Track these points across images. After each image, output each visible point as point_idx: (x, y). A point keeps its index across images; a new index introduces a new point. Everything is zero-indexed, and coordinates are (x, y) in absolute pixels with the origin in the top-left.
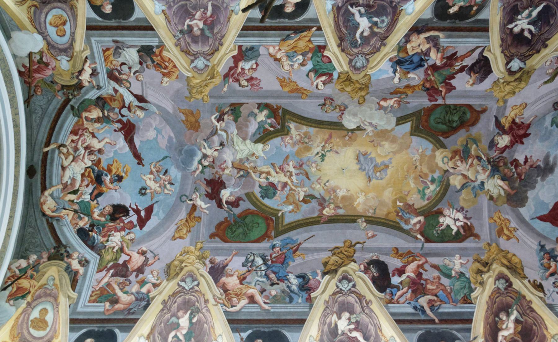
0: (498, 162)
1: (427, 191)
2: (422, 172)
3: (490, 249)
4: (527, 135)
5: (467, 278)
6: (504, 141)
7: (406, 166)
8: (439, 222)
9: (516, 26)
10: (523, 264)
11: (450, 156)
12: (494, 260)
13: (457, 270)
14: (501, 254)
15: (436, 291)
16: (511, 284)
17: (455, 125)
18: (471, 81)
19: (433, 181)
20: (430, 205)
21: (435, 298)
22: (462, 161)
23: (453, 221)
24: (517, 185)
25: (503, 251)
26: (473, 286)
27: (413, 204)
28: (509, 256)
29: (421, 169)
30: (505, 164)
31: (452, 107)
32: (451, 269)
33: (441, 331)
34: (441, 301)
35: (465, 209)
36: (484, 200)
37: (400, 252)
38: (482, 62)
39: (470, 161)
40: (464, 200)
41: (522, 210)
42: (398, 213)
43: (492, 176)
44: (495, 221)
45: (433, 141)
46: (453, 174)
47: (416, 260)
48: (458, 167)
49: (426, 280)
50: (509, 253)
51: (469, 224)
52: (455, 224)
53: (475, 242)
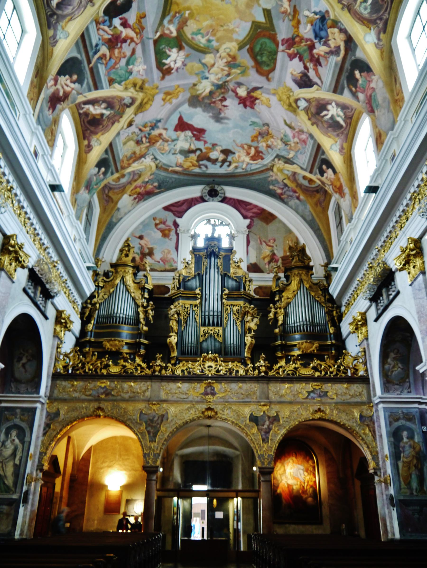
0: (225, 88)
1: (199, 37)
2: (217, 31)
3: (153, 89)
4: (245, 106)
5: (128, 77)
6: (242, 92)
7: (222, 17)
8: (172, 48)
9: (333, 107)
10: (145, 112)
11: (232, 53)
12: (146, 93)
13: (133, 69)
14: (151, 98)
15: (113, 57)
16: (129, 106)
17: (259, 58)
18: (294, 73)
19: (209, 41)
20: (187, 40)
21: (108, 58)
22: (226, 63)
23: (174, 59)
24: (206, 101)
25: (153, 97)
26: (123, 83)
27: (187, 26)
28: (150, 102)
29: (220, 31)
30: (223, 93)
31: (275, 57)
32: (133, 64)
33: (84, 71)
34: (107, 64)
35: (185, 68)
36: (193, 80)
37: (142, 20)
38: (309, 83)
39: (226, 69)
40: (193, 66)
41: (186, 106)
42: (179, 13)
43: (213, 84)
44: (176, 89)
45: (246, 40)
46: (215, 56)
47: (137, 35)
48: (222, 60)
49: (121, 47)
50: (153, 101)
51: (173, 71)
52: (171, 61)
53: (158, 78)
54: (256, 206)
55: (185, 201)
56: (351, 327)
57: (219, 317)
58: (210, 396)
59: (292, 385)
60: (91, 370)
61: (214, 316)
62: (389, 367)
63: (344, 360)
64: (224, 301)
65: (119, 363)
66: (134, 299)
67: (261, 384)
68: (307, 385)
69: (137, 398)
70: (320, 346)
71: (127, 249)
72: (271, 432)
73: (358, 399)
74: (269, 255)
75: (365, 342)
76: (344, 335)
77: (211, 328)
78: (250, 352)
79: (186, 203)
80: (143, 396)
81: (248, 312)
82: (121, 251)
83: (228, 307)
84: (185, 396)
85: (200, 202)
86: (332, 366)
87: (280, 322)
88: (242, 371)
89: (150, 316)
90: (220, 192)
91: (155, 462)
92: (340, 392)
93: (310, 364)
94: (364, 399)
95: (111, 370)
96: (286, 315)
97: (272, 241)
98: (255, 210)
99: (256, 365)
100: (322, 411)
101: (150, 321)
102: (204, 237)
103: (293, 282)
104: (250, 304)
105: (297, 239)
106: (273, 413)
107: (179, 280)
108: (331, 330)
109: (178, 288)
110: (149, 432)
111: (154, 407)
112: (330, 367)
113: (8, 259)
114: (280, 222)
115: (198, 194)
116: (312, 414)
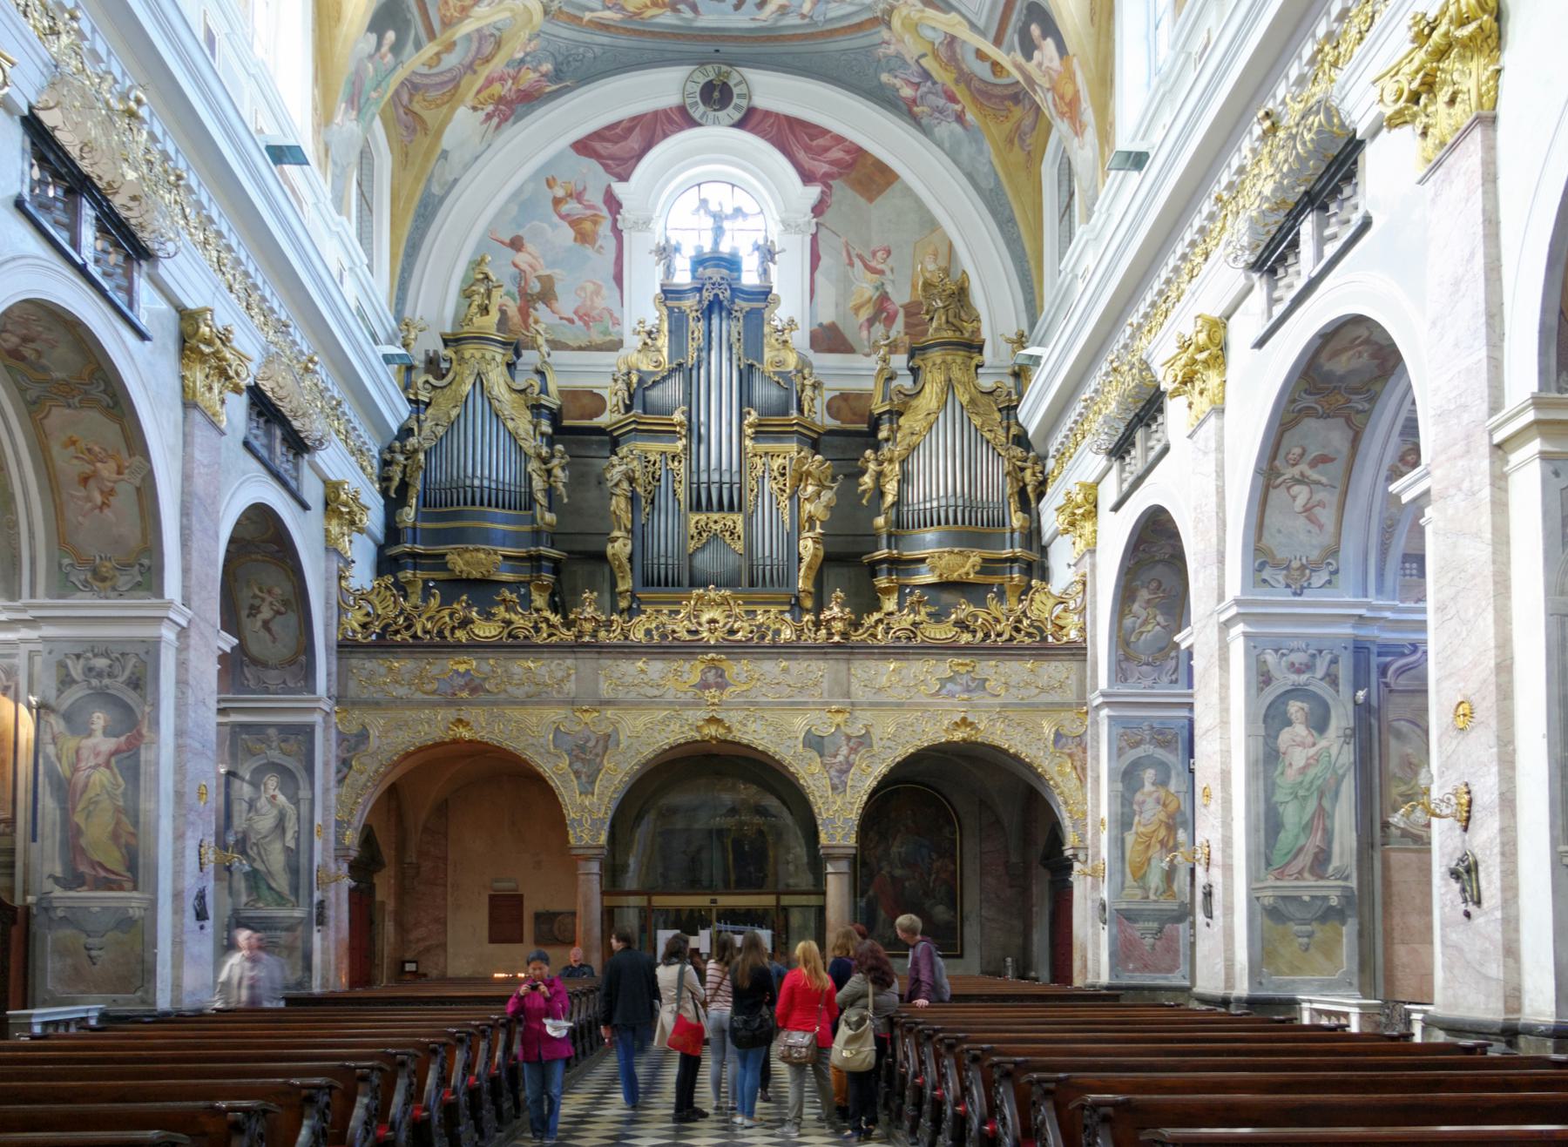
54: (839, 140)
55: (636, 120)
56: (1061, 518)
57: (736, 487)
58: (713, 690)
59: (905, 664)
60: (426, 632)
61: (721, 483)
62: (1135, 623)
63: (1031, 605)
64: (748, 442)
65: (494, 615)
66: (513, 437)
67: (831, 662)
68: (940, 664)
69: (544, 695)
70: (985, 560)
71: (482, 290)
72: (852, 770)
73: (1056, 697)
74: (871, 298)
75: (1087, 556)
76: (1046, 536)
77: (715, 516)
78: (813, 574)
79: (638, 129)
80: (559, 692)
81: (809, 474)
82: (467, 294)
83: (757, 459)
84: (656, 693)
85: (681, 129)
86: (1003, 618)
87: (889, 499)
88: (788, 632)
89: (560, 485)
90: (736, 91)
91: (595, 837)
92: (1014, 680)
93: (951, 614)
94: (1070, 696)
95: (476, 631)
96: (905, 479)
97: (879, 254)
98: (836, 154)
99: (822, 617)
100: (972, 723)
101: (560, 496)
102: (693, 253)
103: (928, 388)
104: (816, 446)
105: (951, 246)
106: (857, 729)
107: (629, 385)
108: (1017, 520)
109: (628, 408)
110: (577, 774)
111: (587, 717)
112: (997, 620)
113: (203, 377)
114: (908, 191)
115: (671, 100)
116: (946, 730)
